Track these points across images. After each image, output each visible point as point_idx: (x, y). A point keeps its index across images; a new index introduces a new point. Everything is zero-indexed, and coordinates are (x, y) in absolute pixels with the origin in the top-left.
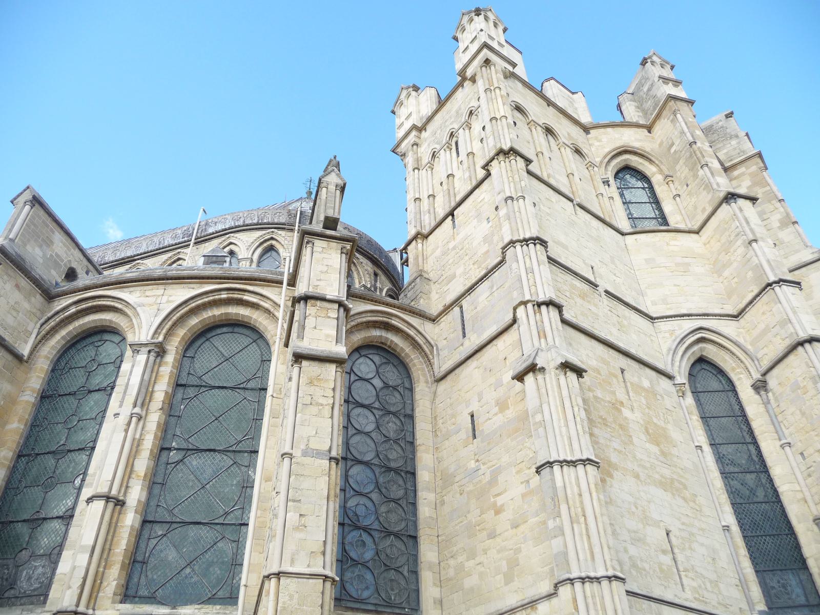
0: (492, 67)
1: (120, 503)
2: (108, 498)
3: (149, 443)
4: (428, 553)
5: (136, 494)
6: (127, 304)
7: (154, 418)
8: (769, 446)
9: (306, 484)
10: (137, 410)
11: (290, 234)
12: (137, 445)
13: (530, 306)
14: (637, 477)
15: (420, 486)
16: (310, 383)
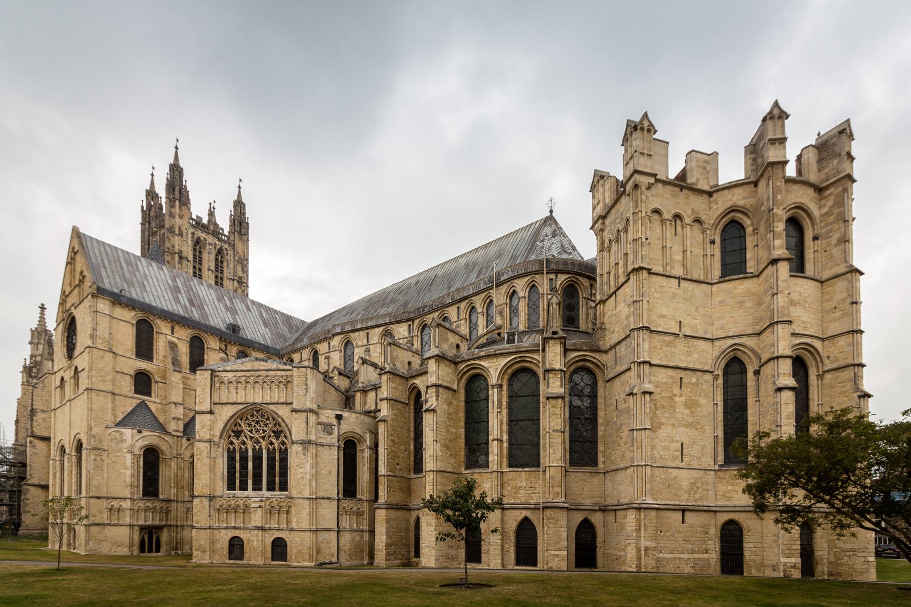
0: (639, 190)
1: (501, 441)
2: (498, 440)
3: (505, 420)
4: (601, 447)
5: (505, 437)
6: (484, 367)
7: (505, 412)
8: (751, 401)
9: (554, 441)
10: (499, 410)
11: (542, 276)
12: (502, 421)
13: (636, 363)
14: (673, 425)
15: (599, 424)
16: (553, 407)
